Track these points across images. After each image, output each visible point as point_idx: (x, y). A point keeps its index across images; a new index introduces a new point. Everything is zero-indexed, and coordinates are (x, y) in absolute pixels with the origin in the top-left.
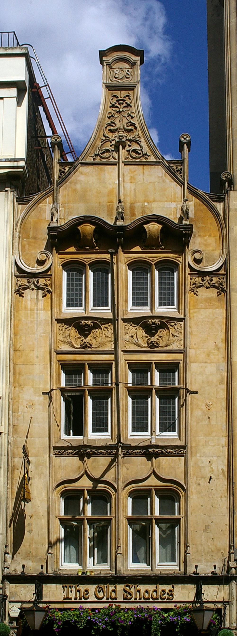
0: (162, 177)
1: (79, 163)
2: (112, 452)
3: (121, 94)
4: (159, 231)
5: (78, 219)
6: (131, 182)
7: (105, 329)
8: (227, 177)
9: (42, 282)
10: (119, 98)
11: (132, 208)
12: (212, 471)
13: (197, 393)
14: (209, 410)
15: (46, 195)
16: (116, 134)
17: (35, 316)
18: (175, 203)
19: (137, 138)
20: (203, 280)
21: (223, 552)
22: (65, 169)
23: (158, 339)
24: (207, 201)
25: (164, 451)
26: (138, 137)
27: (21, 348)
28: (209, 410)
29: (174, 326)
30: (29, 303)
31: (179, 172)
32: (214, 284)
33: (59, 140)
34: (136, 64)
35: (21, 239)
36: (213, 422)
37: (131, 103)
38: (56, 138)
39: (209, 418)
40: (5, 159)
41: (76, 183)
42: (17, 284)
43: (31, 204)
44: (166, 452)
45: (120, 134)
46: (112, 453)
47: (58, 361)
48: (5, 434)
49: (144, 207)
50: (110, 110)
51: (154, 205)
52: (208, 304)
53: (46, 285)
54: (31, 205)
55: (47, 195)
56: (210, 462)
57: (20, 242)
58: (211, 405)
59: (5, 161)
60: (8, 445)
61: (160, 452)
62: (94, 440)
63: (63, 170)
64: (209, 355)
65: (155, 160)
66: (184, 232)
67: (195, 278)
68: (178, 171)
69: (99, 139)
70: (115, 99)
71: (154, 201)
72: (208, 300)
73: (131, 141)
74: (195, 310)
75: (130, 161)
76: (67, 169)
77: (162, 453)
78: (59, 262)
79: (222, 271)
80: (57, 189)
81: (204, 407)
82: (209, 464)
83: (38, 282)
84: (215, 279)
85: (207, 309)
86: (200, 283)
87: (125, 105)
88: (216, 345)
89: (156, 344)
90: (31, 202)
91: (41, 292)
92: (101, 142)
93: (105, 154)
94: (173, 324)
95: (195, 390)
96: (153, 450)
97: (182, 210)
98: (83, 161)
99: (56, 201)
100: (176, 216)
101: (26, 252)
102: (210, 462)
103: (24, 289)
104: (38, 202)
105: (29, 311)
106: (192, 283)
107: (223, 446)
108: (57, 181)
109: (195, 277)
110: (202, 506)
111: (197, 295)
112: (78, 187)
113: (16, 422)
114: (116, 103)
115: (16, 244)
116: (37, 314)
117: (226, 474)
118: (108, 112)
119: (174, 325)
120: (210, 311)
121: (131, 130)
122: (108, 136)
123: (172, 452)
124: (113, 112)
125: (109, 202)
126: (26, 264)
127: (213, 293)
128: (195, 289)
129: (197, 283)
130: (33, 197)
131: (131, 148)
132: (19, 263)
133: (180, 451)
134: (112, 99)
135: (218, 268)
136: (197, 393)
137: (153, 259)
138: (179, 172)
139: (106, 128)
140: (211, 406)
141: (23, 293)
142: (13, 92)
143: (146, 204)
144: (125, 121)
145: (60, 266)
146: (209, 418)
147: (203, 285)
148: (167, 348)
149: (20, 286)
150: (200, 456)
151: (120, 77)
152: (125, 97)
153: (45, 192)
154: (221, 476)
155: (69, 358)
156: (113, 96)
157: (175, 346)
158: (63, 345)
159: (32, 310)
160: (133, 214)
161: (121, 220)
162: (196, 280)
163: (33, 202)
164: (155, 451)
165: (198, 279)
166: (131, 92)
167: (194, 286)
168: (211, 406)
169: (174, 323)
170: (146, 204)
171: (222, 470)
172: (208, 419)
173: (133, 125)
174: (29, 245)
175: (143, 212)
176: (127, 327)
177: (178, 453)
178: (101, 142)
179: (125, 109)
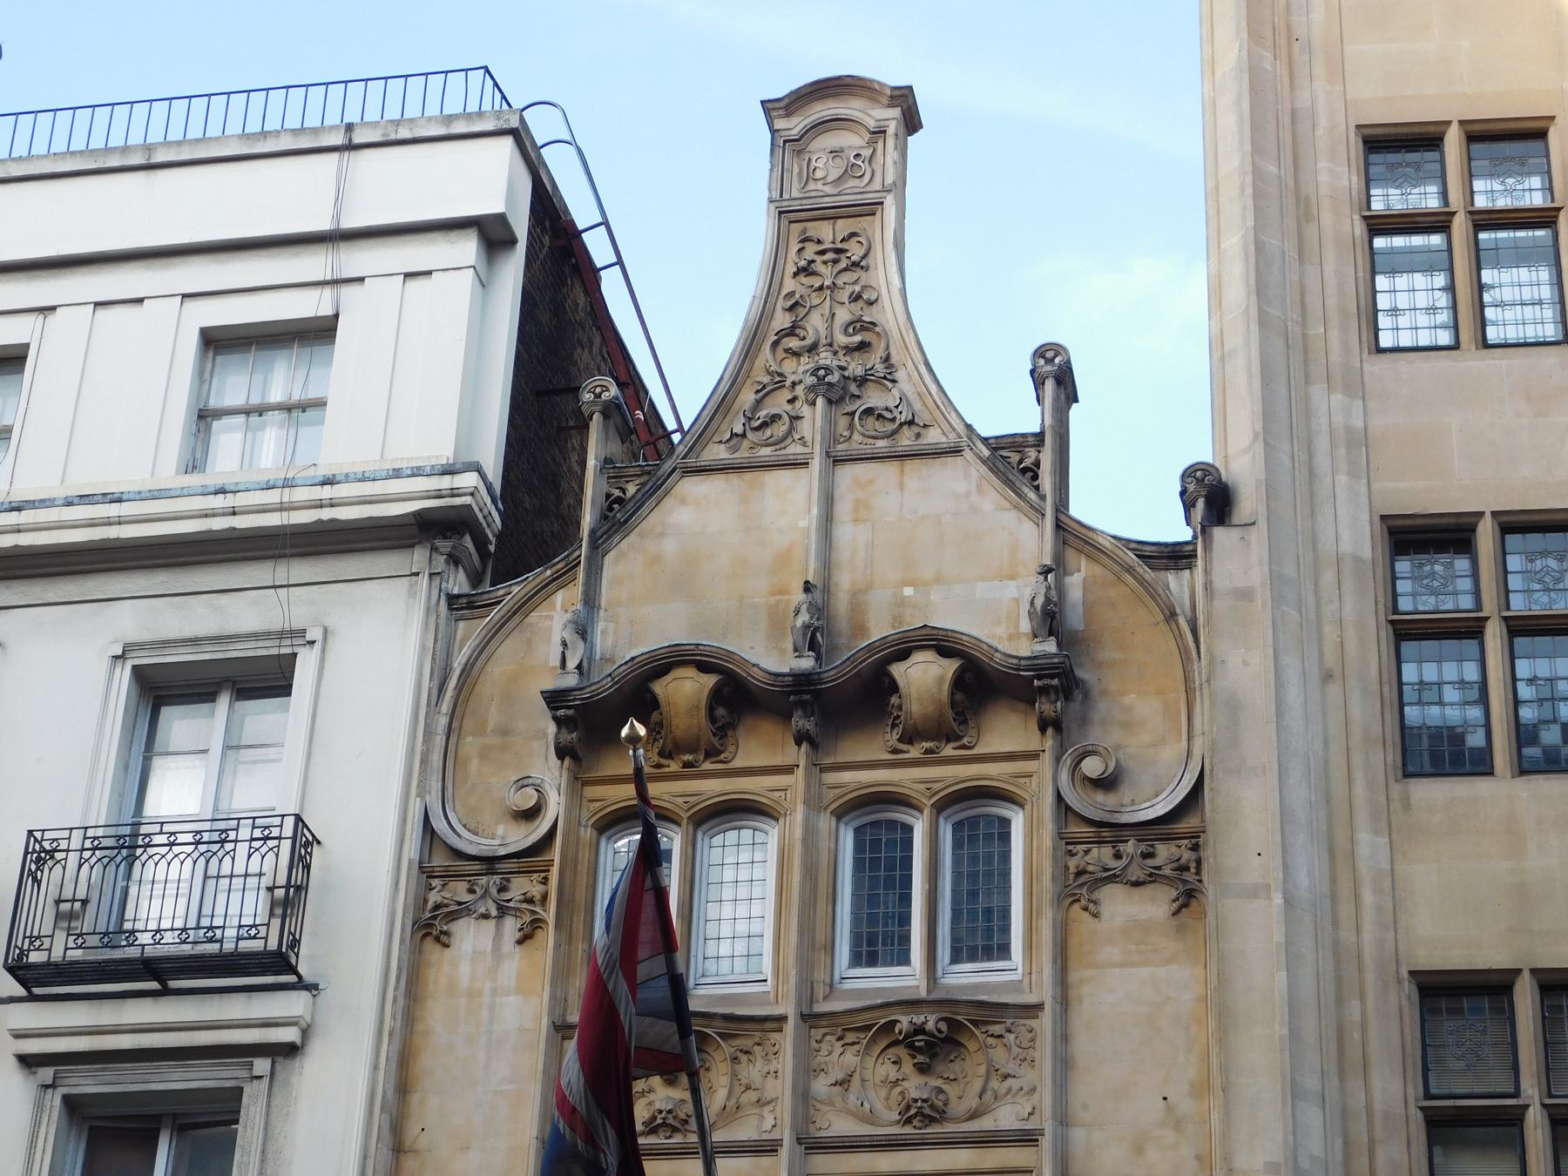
0: (968, 494)
1: (674, 469)
4: (946, 686)
5: (652, 656)
7: (744, 1058)
8: (1203, 480)
9: (521, 886)
10: (827, 245)
11: (857, 607)
15: (555, 580)
16: (806, 363)
17: (485, 1014)
18: (1012, 584)
20: (1118, 856)
22: (624, 491)
23: (940, 1091)
24: (1130, 570)
26: (886, 368)
27: (423, 1142)
29: (1000, 1036)
30: (465, 968)
31: (1030, 474)
32: (1159, 868)
33: (607, 394)
34: (885, 132)
35: (453, 740)
37: (864, 257)
38: (598, 390)
40: (412, 468)
41: (662, 534)
42: (426, 901)
43: (495, 614)
45: (822, 362)
49: (901, 602)
50: (790, 285)
51: (936, 595)
52: (1134, 947)
53: (530, 901)
54: (497, 618)
55: (561, 579)
57: (451, 748)
59: (413, 475)
63: (617, 493)
64: (1139, 1149)
65: (944, 440)
67: (1087, 852)
68: (1024, 471)
69: (749, 381)
71: (938, 580)
73: (862, 381)
75: (855, 446)
76: (631, 489)
78: (585, 814)
79: (1188, 823)
80: (589, 559)
83: (502, 889)
84: (1164, 851)
85: (1132, 965)
86: (1106, 870)
87: (843, 264)
89: (927, 1111)
90: (499, 607)
91: (511, 926)
92: (758, 392)
93: (768, 432)
94: (996, 1029)
97: (1032, 603)
98: (691, 461)
99: (591, 600)
100: (1017, 627)
101: (469, 783)
103: (453, 917)
104: (524, 607)
105: (464, 1000)
106: (1073, 869)
108: (593, 532)
111: (1096, 916)
112: (670, 547)
115: (436, 758)
116: (492, 1008)
118: (784, 292)
119: (1003, 1032)
120: (1145, 972)
121: (863, 346)
122: (779, 371)
124: (800, 291)
125: (774, 594)
126: (464, 826)
127: (1154, 905)
128: (1084, 891)
129: (1090, 868)
130: (507, 589)
131: (858, 403)
132: (439, 825)
134: (800, 250)
135: (1170, 807)
137: (929, 786)
138: (1030, 474)
141: (446, 933)
142: (467, 248)
143: (908, 591)
144: (843, 316)
145: (586, 827)
147: (1115, 876)
148: (974, 1126)
149: (437, 907)
153: (549, 572)
156: (803, 241)
157: (1005, 1118)
159: (473, 994)
160: (860, 629)
161: (807, 653)
162: (1087, 858)
163: (505, 609)
167: (1083, 879)
169: (1003, 1026)
170: (908, 591)
174: (483, 756)
175: (897, 619)
176: (825, 1047)
178: (758, 392)
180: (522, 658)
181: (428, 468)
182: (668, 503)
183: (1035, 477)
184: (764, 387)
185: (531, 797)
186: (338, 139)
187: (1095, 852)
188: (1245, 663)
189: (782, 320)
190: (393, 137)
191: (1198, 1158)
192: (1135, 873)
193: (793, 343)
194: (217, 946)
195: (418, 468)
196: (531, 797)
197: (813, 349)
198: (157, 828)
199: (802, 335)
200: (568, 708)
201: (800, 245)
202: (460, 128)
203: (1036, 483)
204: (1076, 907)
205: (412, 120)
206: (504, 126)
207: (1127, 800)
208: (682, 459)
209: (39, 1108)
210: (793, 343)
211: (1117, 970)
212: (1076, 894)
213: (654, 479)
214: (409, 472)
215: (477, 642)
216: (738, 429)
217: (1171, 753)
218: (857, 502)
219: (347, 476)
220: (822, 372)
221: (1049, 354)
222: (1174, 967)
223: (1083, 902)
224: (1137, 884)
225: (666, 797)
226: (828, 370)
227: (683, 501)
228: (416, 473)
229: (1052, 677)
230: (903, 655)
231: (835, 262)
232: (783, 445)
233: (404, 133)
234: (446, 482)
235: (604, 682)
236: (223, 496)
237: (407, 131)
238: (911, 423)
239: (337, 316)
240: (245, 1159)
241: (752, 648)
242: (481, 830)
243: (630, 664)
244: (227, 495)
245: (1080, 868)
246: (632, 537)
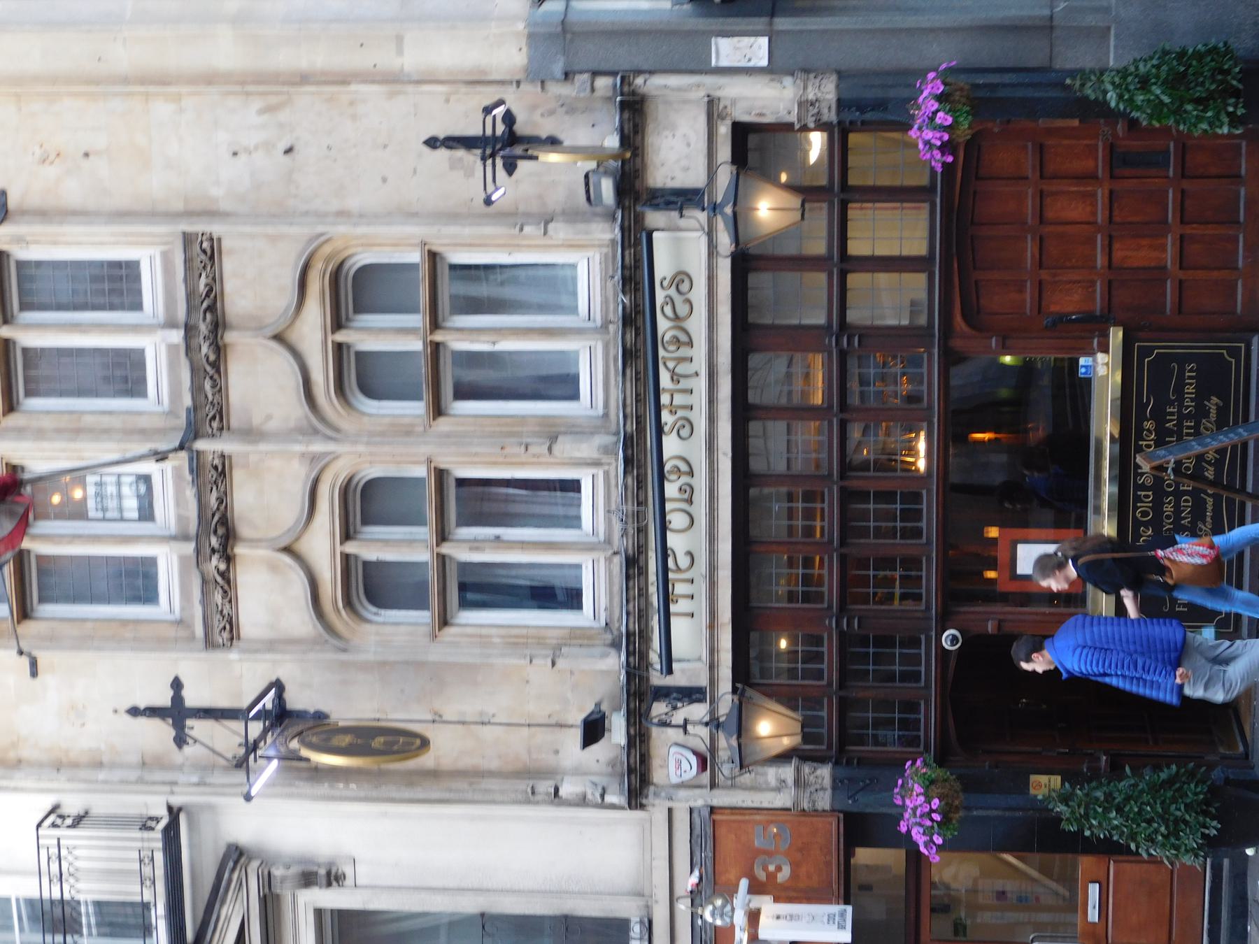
2: (216, 468)
12: (268, 146)
21: (539, 112)
25: (205, 305)
39: (87, 155)
44: (207, 295)
46: (220, 469)
48: (172, 793)
56: (235, 154)
60: (205, 784)
61: (208, 316)
62: (181, 519)
77: (211, 308)
81: (51, 172)
82: (243, 157)
102: (235, 154)
110: (384, 180)
117: (273, 100)
133: (204, 251)
154: (283, 116)
171: (262, 111)
172: (91, 157)
177: (212, 258)
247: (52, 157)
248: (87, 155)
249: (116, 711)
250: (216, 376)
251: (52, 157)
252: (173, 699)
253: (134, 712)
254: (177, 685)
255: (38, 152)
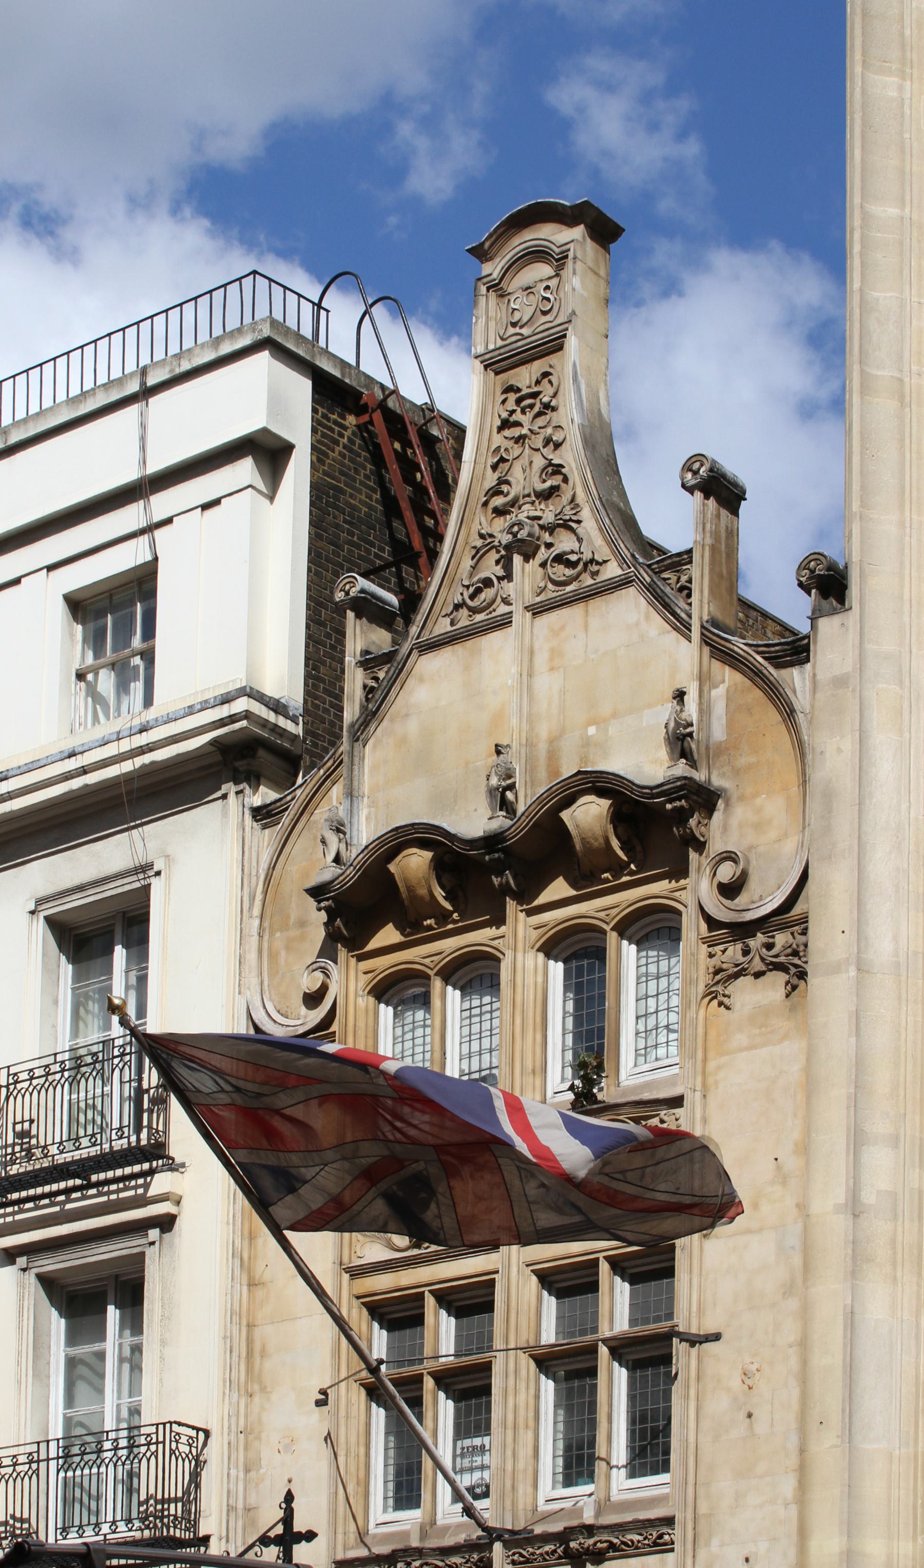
0: (637, 624)
1: (412, 650)
3: (524, 377)
6: (552, 669)
10: (525, 391)
13: (717, 1337)
14: (750, 1388)
19: (568, 513)
27: (267, 1277)
28: (750, 1388)
31: (686, 592)
36: (761, 1426)
37: (555, 395)
41: (407, 715)
47: (358, 1298)
49: (587, 743)
52: (757, 1031)
58: (758, 1370)
61: (605, 1545)
66: (669, 806)
67: (724, 952)
70: (512, 397)
71: (614, 715)
72: (760, 1018)
73: (551, 529)
74: (723, 1060)
77: (612, 1546)
78: (361, 984)
81: (735, 1382)
84: (781, 939)
88: (779, 1168)
93: (483, 596)
95: (712, 1330)
96: (580, 1544)
98: (425, 636)
107: (786, 1505)
109: (721, 947)
111: (728, 1008)
113: (252, 1500)
114: (512, 412)
115: (252, 956)
120: (763, 1052)
123: (639, 1541)
129: (725, 966)
133: (660, 1536)
134: (504, 402)
136: (717, 1337)
138: (686, 592)
139: (485, 504)
140: (758, 1375)
143: (592, 730)
144: (539, 462)
146: (750, 1415)
150: (722, 1545)
151: (525, 320)
152: (538, 382)
155: (383, 1282)
158: (368, 1245)
164: (586, 1545)
165: (734, 951)
166: (553, 359)
167: (718, 977)
168: (758, 1375)
170: (592, 730)
172: (748, 1420)
173: (557, 469)
174: (288, 948)
177: (655, 1544)
179: (541, 421)
180: (311, 854)
181: (212, 700)
182: (410, 682)
183: (689, 596)
184: (477, 552)
185: (318, 979)
186: (133, 387)
187: (731, 949)
188: (839, 750)
189: (491, 479)
190: (178, 371)
191: (798, 1206)
192: (758, 965)
193: (498, 501)
194: (98, 1147)
195: (206, 701)
196: (318, 979)
197: (514, 503)
198: (51, 1060)
199: (505, 491)
200: (327, 899)
201: (504, 396)
202: (227, 348)
203: (689, 601)
204: (715, 1002)
205: (189, 350)
206: (259, 337)
207: (756, 897)
208: (417, 639)
209: (21, 1286)
210: (498, 501)
211: (744, 1054)
212: (713, 992)
213: (395, 664)
214: (199, 707)
215: (275, 847)
216: (458, 599)
217: (790, 846)
218: (552, 650)
219: (156, 720)
220: (516, 529)
221: (696, 466)
222: (786, 1043)
223: (720, 998)
224: (758, 975)
225: (418, 960)
226: (520, 524)
227: (421, 680)
228: (205, 706)
229: (679, 799)
230: (569, 801)
231: (531, 406)
232: (491, 609)
233: (186, 366)
234: (224, 711)
235: (348, 872)
236: (74, 758)
237: (187, 362)
238: (592, 561)
239: (156, 559)
240: (150, 1306)
241: (476, 810)
242: (289, 1013)
243: (365, 852)
244: (78, 756)
245: (717, 967)
246: (385, 723)
247: (748, 1382)
248: (750, 1415)
249: (290, 1481)
250: (556, 1555)
251: (748, 1382)
252: (300, 1533)
253: (289, 1498)
254: (310, 1536)
255: (754, 1368)
